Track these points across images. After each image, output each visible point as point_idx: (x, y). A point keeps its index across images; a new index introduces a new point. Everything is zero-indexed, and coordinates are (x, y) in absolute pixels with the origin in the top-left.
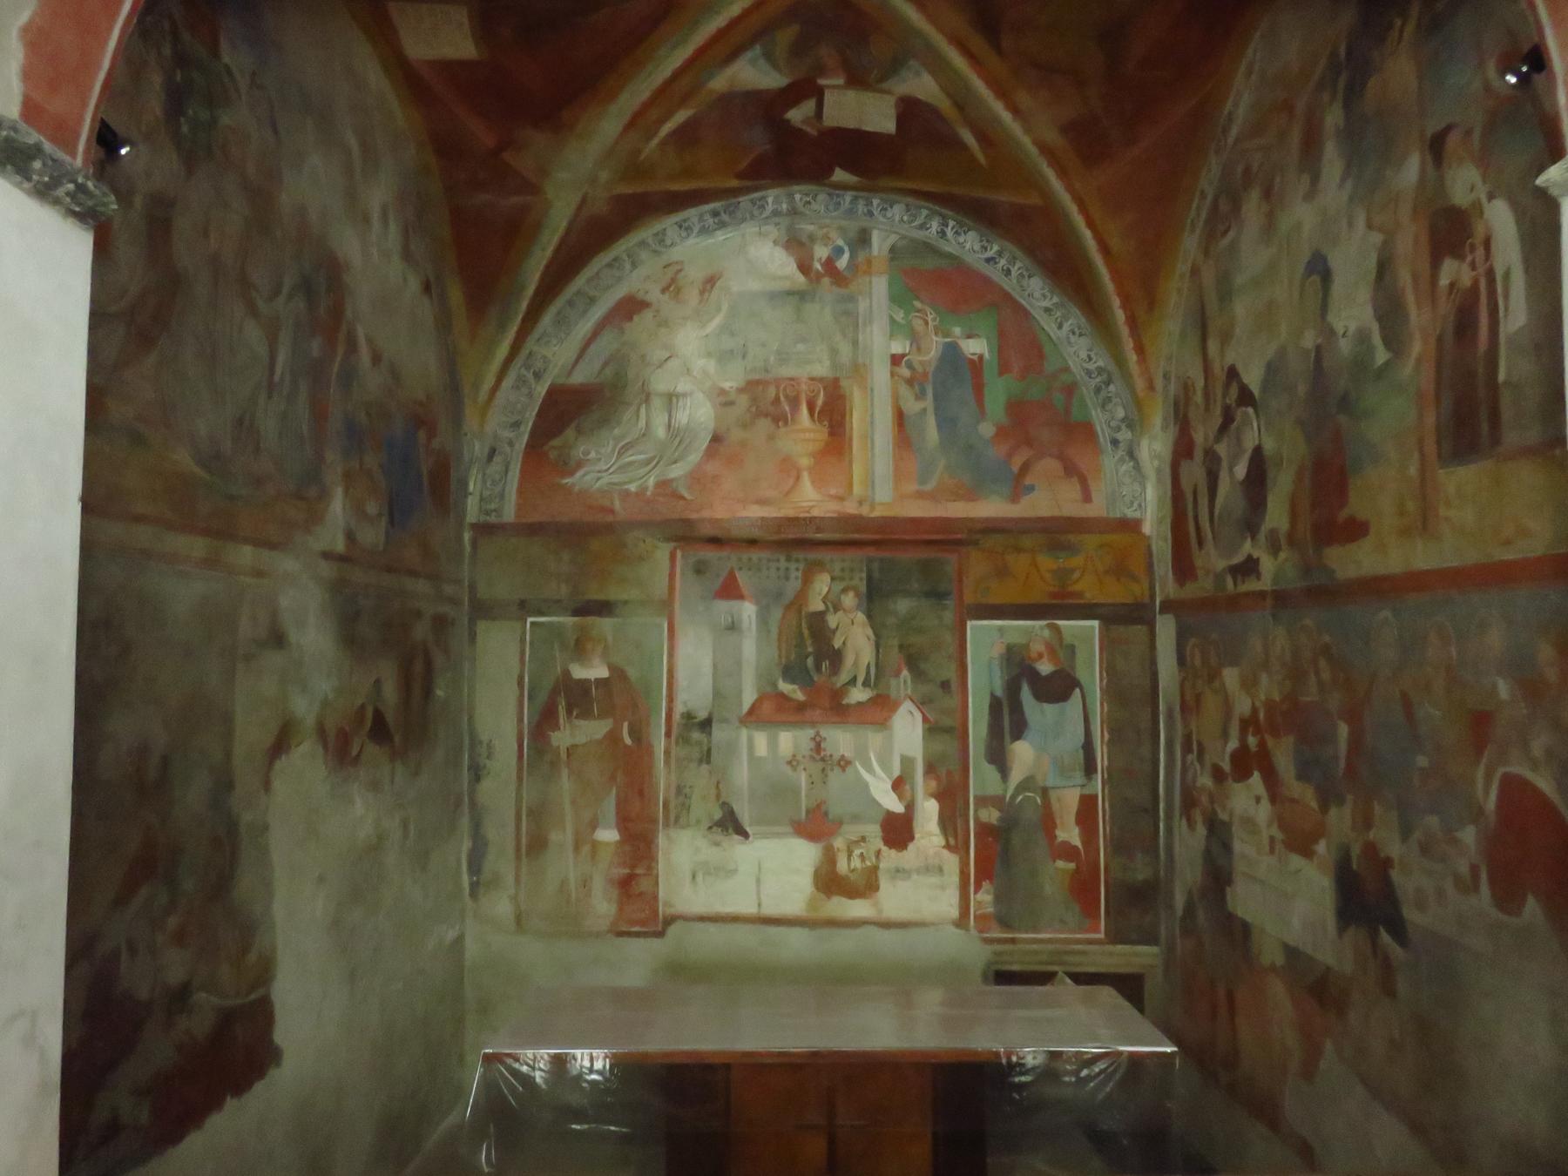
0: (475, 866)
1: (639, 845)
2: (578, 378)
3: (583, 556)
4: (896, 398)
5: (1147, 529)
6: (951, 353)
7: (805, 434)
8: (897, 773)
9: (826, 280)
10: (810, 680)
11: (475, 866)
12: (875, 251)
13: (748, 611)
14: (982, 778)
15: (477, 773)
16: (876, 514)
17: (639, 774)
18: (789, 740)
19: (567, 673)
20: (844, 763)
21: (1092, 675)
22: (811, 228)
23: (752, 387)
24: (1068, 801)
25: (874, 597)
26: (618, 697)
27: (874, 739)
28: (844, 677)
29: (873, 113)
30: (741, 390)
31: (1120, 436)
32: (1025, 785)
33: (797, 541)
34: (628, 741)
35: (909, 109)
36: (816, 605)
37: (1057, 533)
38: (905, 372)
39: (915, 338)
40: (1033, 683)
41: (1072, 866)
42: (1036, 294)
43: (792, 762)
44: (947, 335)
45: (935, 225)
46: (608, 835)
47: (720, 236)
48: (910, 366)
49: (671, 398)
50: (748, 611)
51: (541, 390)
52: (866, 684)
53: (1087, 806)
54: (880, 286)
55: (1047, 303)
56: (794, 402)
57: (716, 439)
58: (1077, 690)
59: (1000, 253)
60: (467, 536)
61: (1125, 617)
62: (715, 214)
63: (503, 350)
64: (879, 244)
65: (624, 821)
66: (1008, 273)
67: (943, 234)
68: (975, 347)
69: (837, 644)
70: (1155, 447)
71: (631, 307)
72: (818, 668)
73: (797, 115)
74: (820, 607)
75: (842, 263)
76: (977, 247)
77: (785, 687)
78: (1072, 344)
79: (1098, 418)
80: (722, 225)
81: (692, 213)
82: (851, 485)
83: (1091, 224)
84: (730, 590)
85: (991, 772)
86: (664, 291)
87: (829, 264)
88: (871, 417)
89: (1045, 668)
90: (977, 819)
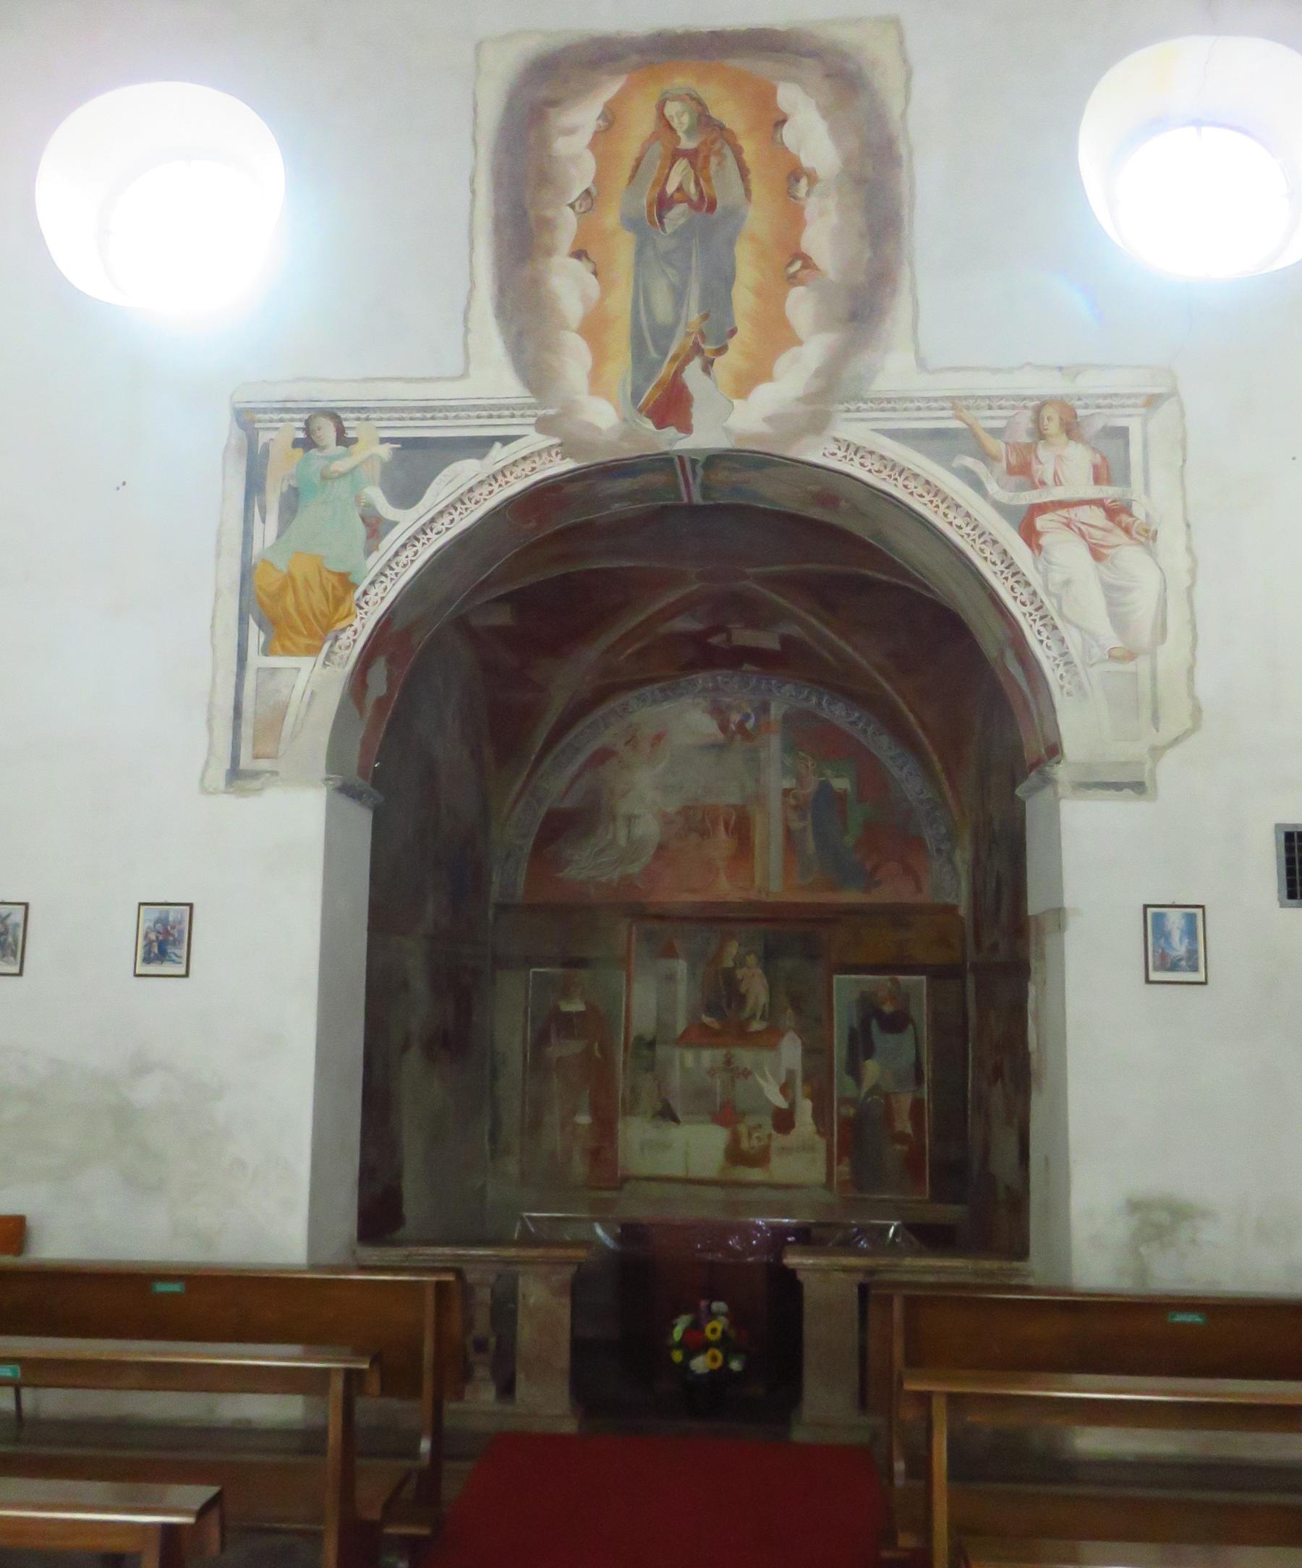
0: (493, 1138)
1: (605, 1128)
2: (567, 804)
3: (573, 931)
4: (786, 820)
5: (963, 911)
6: (825, 787)
7: (722, 843)
8: (783, 1081)
9: (738, 737)
10: (723, 1017)
11: (493, 1138)
12: (772, 717)
13: (681, 967)
14: (843, 1085)
15: (494, 1075)
16: (771, 899)
17: (607, 1073)
18: (709, 1057)
19: (558, 1008)
20: (746, 1074)
21: (921, 1012)
22: (728, 700)
23: (686, 811)
24: (904, 1103)
25: (769, 957)
26: (595, 1024)
27: (766, 1056)
28: (746, 1014)
29: (768, 641)
30: (679, 813)
31: (943, 847)
32: (875, 1089)
33: (716, 918)
34: (597, 1054)
35: (786, 641)
36: (729, 963)
37: (898, 915)
38: (792, 802)
39: (800, 780)
40: (878, 1019)
41: (906, 1148)
42: (884, 747)
43: (712, 1072)
44: (822, 775)
45: (814, 700)
46: (584, 1119)
47: (666, 706)
48: (795, 797)
49: (630, 819)
50: (681, 967)
51: (543, 812)
52: (762, 1018)
53: (917, 1107)
54: (774, 745)
55: (892, 754)
56: (715, 823)
57: (661, 847)
58: (911, 1027)
59: (859, 718)
60: (491, 913)
61: (943, 974)
62: (662, 690)
63: (517, 787)
64: (776, 712)
65: (595, 1110)
66: (865, 731)
67: (820, 704)
68: (841, 784)
69: (743, 990)
70: (963, 857)
71: (603, 756)
72: (729, 1006)
73: (715, 640)
74: (731, 964)
75: (750, 725)
76: (844, 714)
77: (706, 1019)
78: (909, 782)
79: (928, 834)
80: (666, 698)
81: (647, 689)
82: (753, 881)
83: (912, 711)
84: (670, 953)
85: (849, 1081)
86: (627, 743)
87: (741, 725)
88: (769, 831)
89: (888, 1008)
90: (839, 1115)
